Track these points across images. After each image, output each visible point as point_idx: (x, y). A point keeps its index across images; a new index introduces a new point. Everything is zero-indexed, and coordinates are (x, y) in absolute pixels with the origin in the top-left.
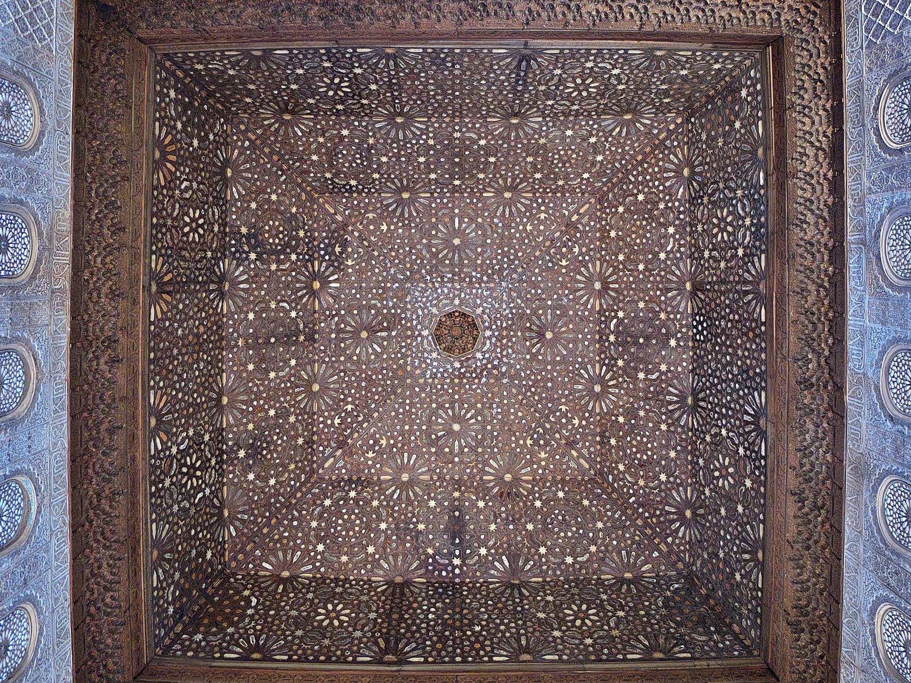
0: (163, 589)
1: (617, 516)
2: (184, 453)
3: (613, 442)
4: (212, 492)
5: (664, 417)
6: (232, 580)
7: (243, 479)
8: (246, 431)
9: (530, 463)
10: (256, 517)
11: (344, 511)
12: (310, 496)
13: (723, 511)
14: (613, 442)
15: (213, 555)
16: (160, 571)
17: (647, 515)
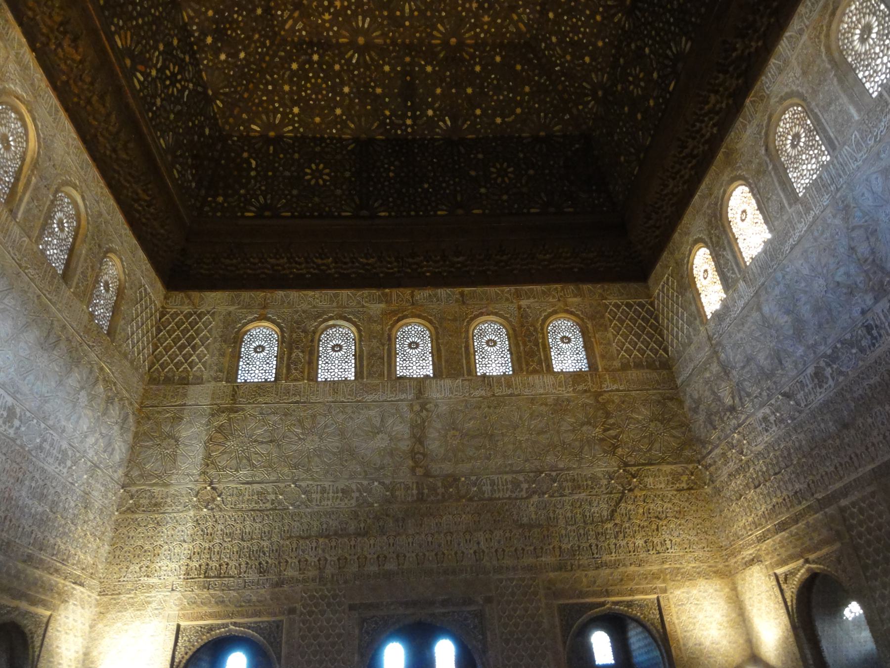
0: (184, 175)
1: (543, 81)
2: (161, 71)
3: (551, 15)
4: (194, 84)
5: (601, 9)
6: (230, 142)
7: (216, 61)
8: (208, 19)
9: (473, 27)
10: (235, 88)
11: (311, 75)
12: (277, 59)
13: (626, 109)
14: (551, 15)
15: (210, 129)
16: (178, 166)
17: (567, 83)
